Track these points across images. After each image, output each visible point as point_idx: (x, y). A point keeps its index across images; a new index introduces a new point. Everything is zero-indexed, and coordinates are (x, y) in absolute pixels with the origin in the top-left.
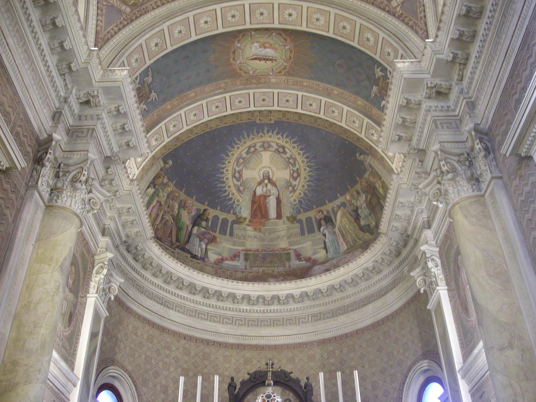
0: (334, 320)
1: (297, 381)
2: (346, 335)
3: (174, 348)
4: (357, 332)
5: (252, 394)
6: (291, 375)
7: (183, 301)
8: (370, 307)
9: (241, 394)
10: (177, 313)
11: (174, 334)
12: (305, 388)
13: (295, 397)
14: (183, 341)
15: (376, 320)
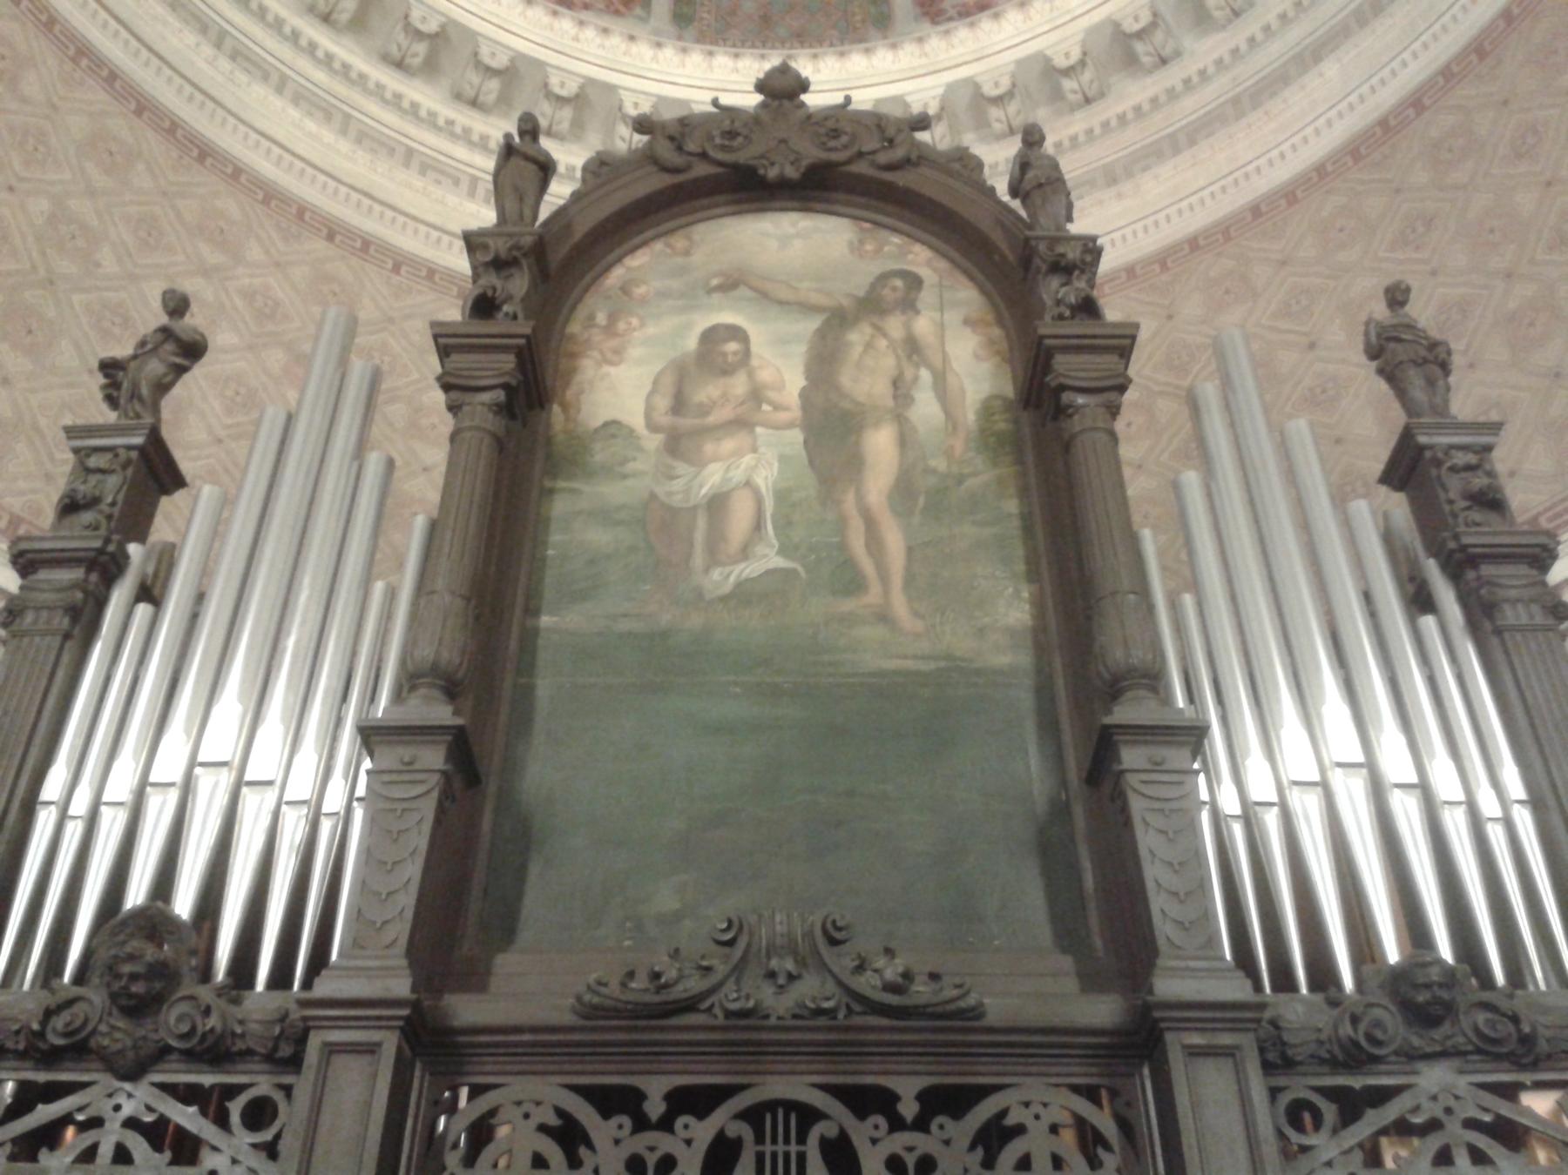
0: (1120, 196)
1: (964, 165)
2: (1194, 244)
3: (254, 253)
4: (1255, 210)
5: (658, 246)
6: (923, 136)
7: (341, 89)
8: (1331, 69)
9: (582, 227)
10: (294, 113)
11: (270, 196)
12: (1014, 191)
13: (943, 264)
14: (319, 246)
15: (1375, 115)
